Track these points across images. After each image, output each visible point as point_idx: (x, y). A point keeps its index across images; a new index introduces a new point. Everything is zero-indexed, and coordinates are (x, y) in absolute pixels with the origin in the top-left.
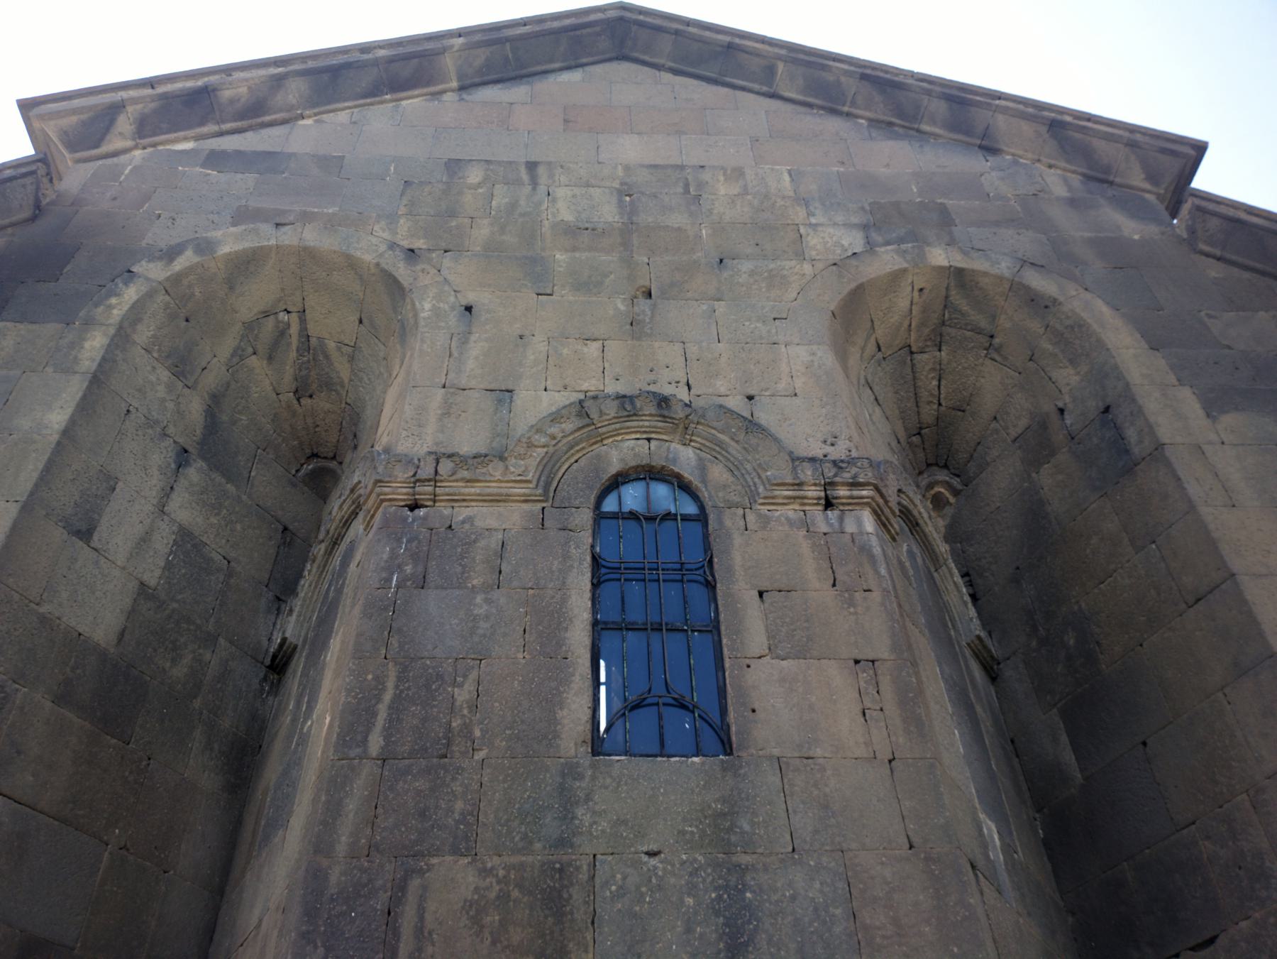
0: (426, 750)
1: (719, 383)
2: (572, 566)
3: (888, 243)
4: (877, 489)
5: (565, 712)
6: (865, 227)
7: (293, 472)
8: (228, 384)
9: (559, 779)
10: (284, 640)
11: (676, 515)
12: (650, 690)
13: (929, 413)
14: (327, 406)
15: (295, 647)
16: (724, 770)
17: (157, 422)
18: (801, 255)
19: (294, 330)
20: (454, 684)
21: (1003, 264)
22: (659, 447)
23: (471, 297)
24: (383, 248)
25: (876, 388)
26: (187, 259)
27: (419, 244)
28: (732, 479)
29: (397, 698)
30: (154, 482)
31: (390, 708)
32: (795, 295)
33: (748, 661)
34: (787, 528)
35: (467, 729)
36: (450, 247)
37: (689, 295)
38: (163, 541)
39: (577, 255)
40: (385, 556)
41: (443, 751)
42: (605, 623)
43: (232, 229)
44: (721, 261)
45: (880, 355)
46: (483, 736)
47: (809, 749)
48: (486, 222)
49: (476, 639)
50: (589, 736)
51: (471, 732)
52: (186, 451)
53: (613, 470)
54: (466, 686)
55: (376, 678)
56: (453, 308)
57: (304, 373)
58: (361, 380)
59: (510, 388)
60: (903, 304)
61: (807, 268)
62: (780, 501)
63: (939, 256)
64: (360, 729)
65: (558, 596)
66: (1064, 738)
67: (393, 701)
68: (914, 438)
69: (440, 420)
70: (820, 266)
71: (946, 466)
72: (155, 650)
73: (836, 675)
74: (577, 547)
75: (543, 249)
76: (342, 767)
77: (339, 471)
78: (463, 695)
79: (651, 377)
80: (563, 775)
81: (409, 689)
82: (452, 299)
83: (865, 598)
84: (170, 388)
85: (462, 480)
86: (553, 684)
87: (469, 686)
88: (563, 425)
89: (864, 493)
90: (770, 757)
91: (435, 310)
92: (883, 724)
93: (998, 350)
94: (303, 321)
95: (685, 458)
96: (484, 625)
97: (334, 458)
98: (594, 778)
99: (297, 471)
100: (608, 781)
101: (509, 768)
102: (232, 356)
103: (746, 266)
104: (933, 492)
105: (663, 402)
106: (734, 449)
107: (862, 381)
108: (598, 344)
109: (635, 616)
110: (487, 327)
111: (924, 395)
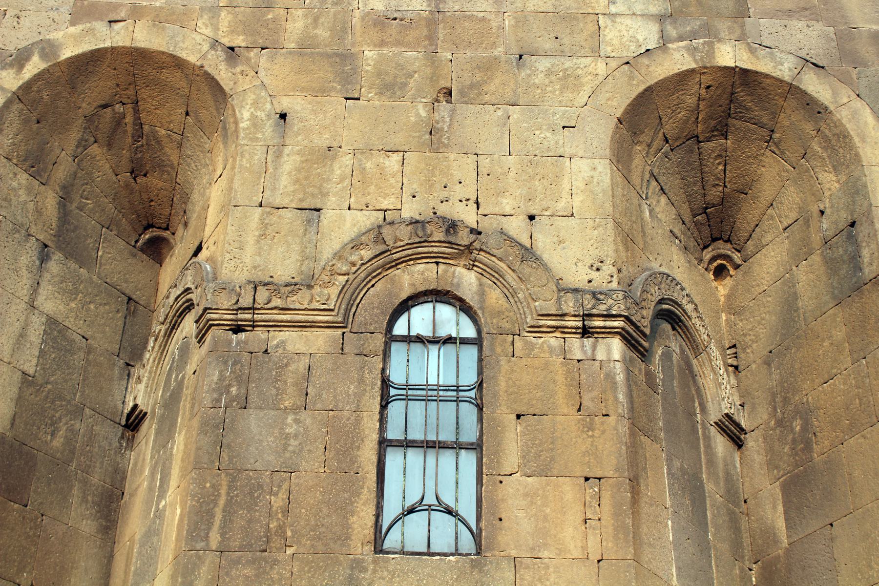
0: (251, 545)
1: (505, 201)
2: (365, 390)
3: (681, 39)
4: (627, 319)
5: (355, 518)
6: (661, 19)
7: (133, 243)
8: (75, 174)
9: (349, 571)
10: (135, 406)
11: (456, 338)
12: (422, 499)
13: (714, 194)
14: (161, 184)
15: (146, 413)
16: (473, 567)
17: (22, 225)
18: (596, 52)
19: (129, 119)
20: (271, 493)
21: (786, 65)
22: (446, 271)
23: (285, 103)
24: (206, 47)
25: (661, 179)
26: (35, 66)
27: (239, 41)
28: (506, 305)
29: (229, 502)
30: (25, 281)
31: (224, 511)
32: (585, 98)
33: (500, 478)
34: (547, 355)
35: (281, 529)
36: (266, 45)
37: (487, 98)
38: (35, 334)
39: (385, 50)
40: (215, 378)
41: (264, 547)
42: (390, 441)
43: (72, 29)
44: (521, 56)
45: (667, 148)
46: (293, 537)
47: (539, 551)
48: (300, 12)
49: (288, 455)
50: (373, 538)
51: (285, 532)
52: (46, 246)
53: (404, 296)
54: (280, 495)
55: (213, 486)
56: (269, 116)
57: (139, 155)
58: (189, 165)
59: (318, 206)
60: (691, 101)
61: (601, 68)
62: (545, 329)
63: (728, 55)
64: (203, 527)
65: (353, 418)
66: (780, 508)
67: (226, 506)
68: (699, 217)
69: (258, 242)
70: (613, 64)
71: (728, 241)
72: (39, 428)
73: (569, 490)
74: (371, 372)
75: (353, 44)
76: (192, 556)
77: (172, 241)
78: (278, 502)
79: (444, 194)
80: (352, 568)
81: (237, 496)
82: (268, 106)
83: (602, 423)
84: (29, 190)
85: (275, 308)
86: (346, 495)
87: (283, 495)
88: (362, 252)
89: (616, 324)
90: (508, 557)
91: (253, 117)
92: (599, 532)
93: (777, 145)
94: (136, 111)
95: (467, 281)
96: (292, 442)
97: (167, 229)
98: (375, 571)
99: (137, 242)
100: (386, 573)
101: (312, 562)
102: (77, 147)
103: (543, 64)
104: (715, 264)
105: (452, 226)
106: (510, 277)
107: (647, 176)
108: (396, 157)
109: (416, 434)
110: (300, 138)
111: (711, 179)
